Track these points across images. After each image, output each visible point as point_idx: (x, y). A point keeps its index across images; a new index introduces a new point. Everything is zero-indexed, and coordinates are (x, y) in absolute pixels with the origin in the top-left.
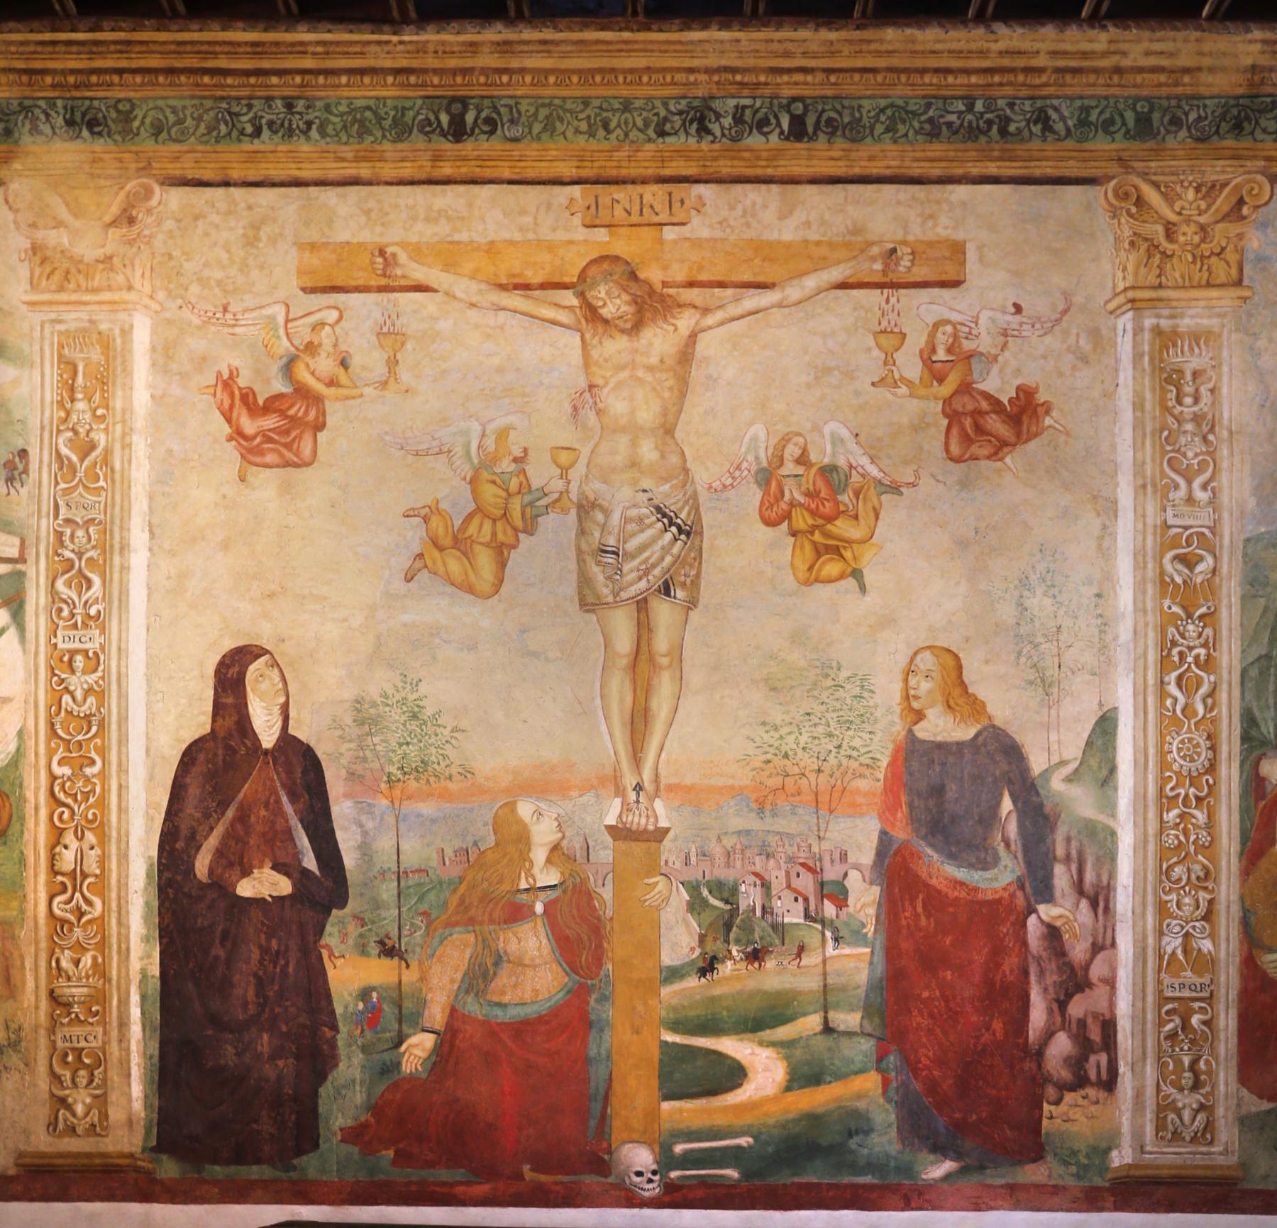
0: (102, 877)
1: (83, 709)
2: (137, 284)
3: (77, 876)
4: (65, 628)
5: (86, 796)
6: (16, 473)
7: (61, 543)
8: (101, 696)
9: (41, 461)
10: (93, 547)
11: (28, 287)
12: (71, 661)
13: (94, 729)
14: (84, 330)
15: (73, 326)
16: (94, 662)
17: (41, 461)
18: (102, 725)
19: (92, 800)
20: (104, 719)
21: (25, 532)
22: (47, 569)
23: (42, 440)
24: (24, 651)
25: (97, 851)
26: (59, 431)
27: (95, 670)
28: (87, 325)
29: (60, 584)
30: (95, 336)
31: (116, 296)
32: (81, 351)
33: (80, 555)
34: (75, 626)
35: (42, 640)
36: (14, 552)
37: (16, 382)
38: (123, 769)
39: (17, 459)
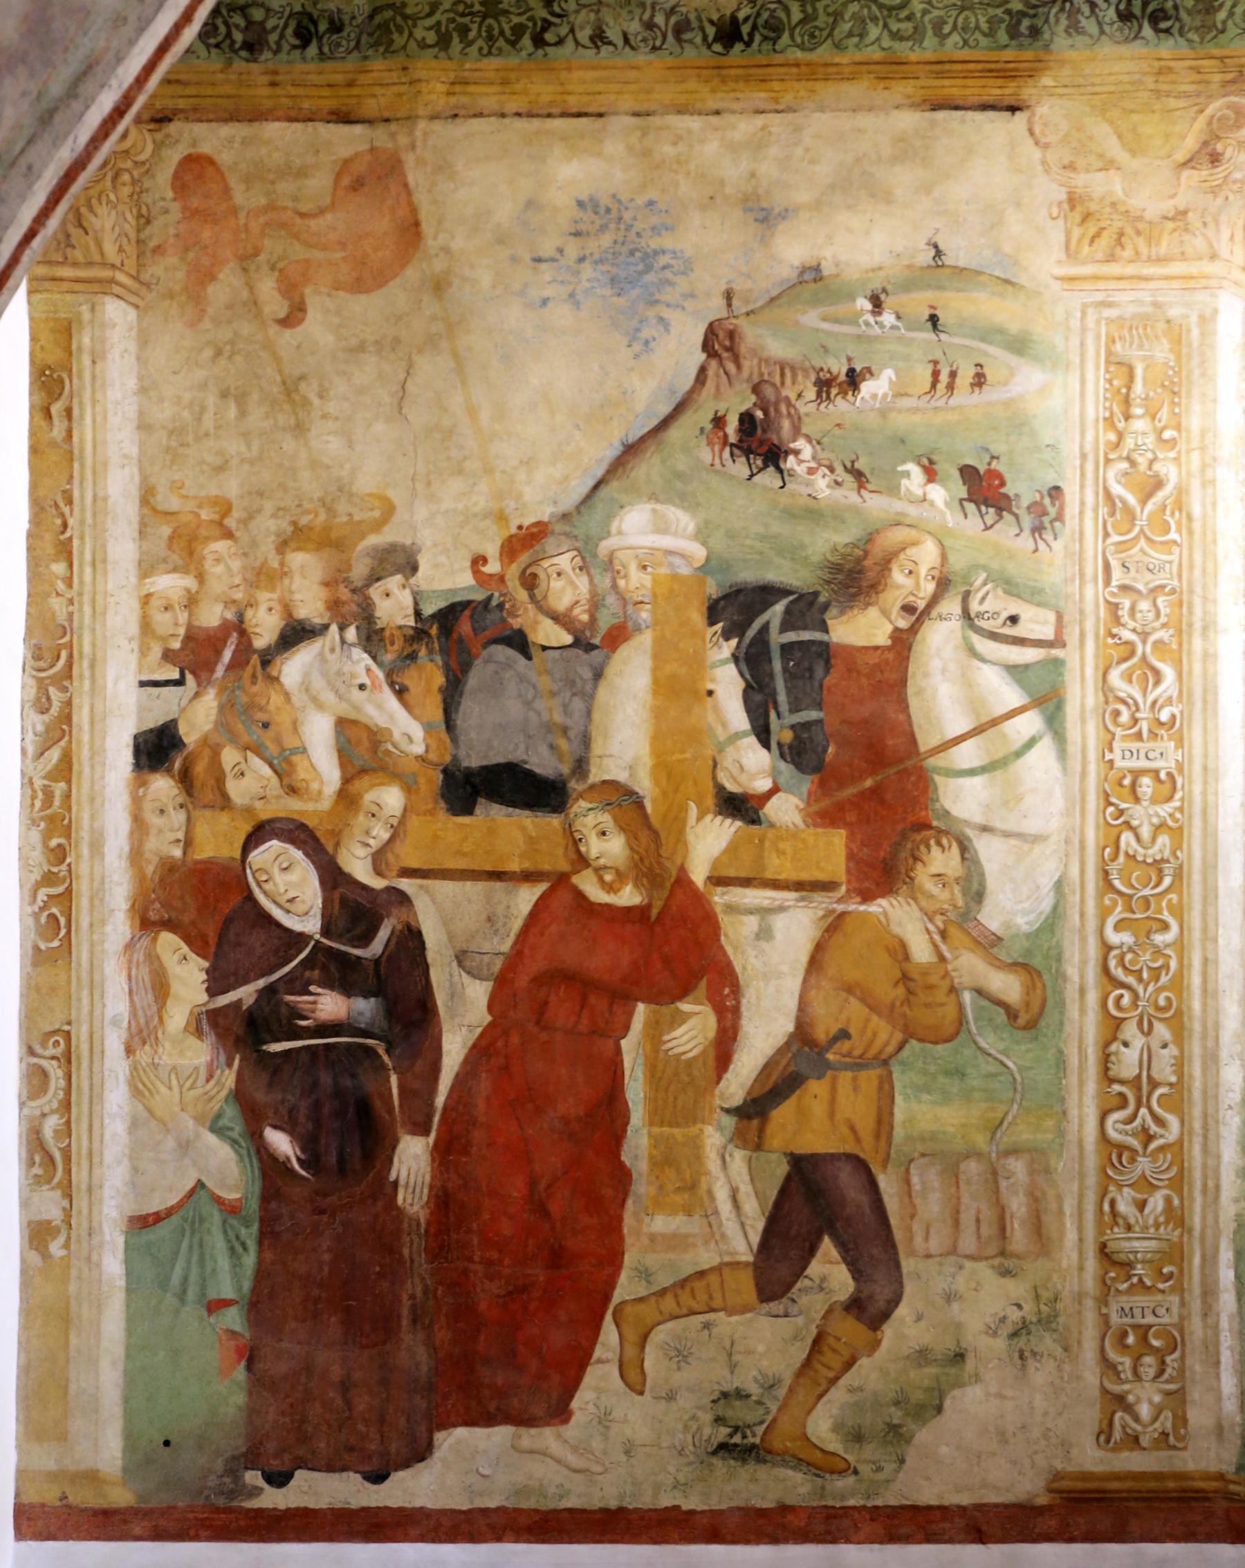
0: (1180, 1085)
1: (1151, 852)
2: (1223, 249)
3: (1143, 1085)
4: (1125, 738)
5: (1156, 973)
6: (1046, 520)
7: (1117, 620)
8: (1178, 833)
9: (1082, 503)
10: (1164, 625)
11: (1063, 256)
12: (1134, 785)
13: (1167, 881)
14: (1145, 317)
15: (1130, 310)
16: (1168, 786)
17: (1082, 503)
18: (1178, 874)
19: (1164, 979)
20: (1181, 867)
21: (1062, 603)
22: (1097, 656)
23: (1083, 475)
24: (1065, 770)
25: (1173, 1050)
26: (1108, 461)
27: (1170, 798)
28: (1150, 309)
29: (1115, 678)
30: (1161, 326)
31: (1193, 268)
32: (1141, 347)
33: (1144, 636)
34: (1139, 736)
35: (1092, 756)
36: (1048, 633)
37: (1044, 391)
38: (1209, 938)
39: (1047, 501)
